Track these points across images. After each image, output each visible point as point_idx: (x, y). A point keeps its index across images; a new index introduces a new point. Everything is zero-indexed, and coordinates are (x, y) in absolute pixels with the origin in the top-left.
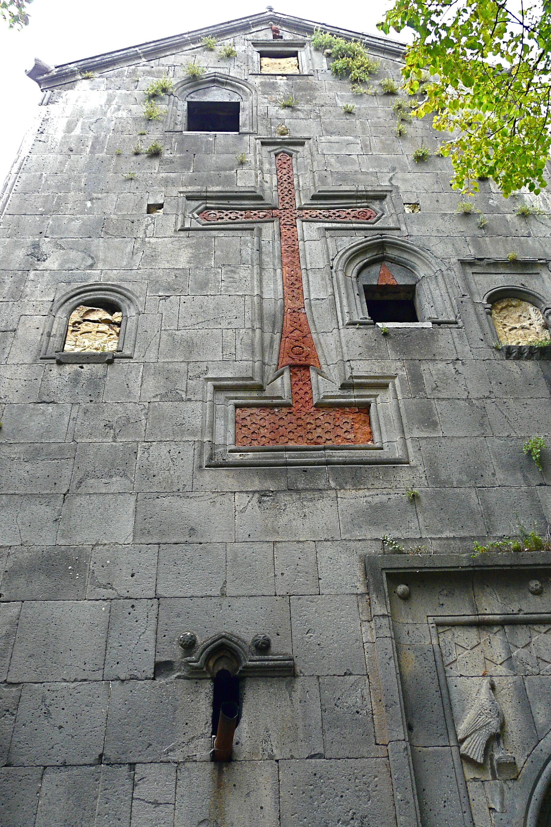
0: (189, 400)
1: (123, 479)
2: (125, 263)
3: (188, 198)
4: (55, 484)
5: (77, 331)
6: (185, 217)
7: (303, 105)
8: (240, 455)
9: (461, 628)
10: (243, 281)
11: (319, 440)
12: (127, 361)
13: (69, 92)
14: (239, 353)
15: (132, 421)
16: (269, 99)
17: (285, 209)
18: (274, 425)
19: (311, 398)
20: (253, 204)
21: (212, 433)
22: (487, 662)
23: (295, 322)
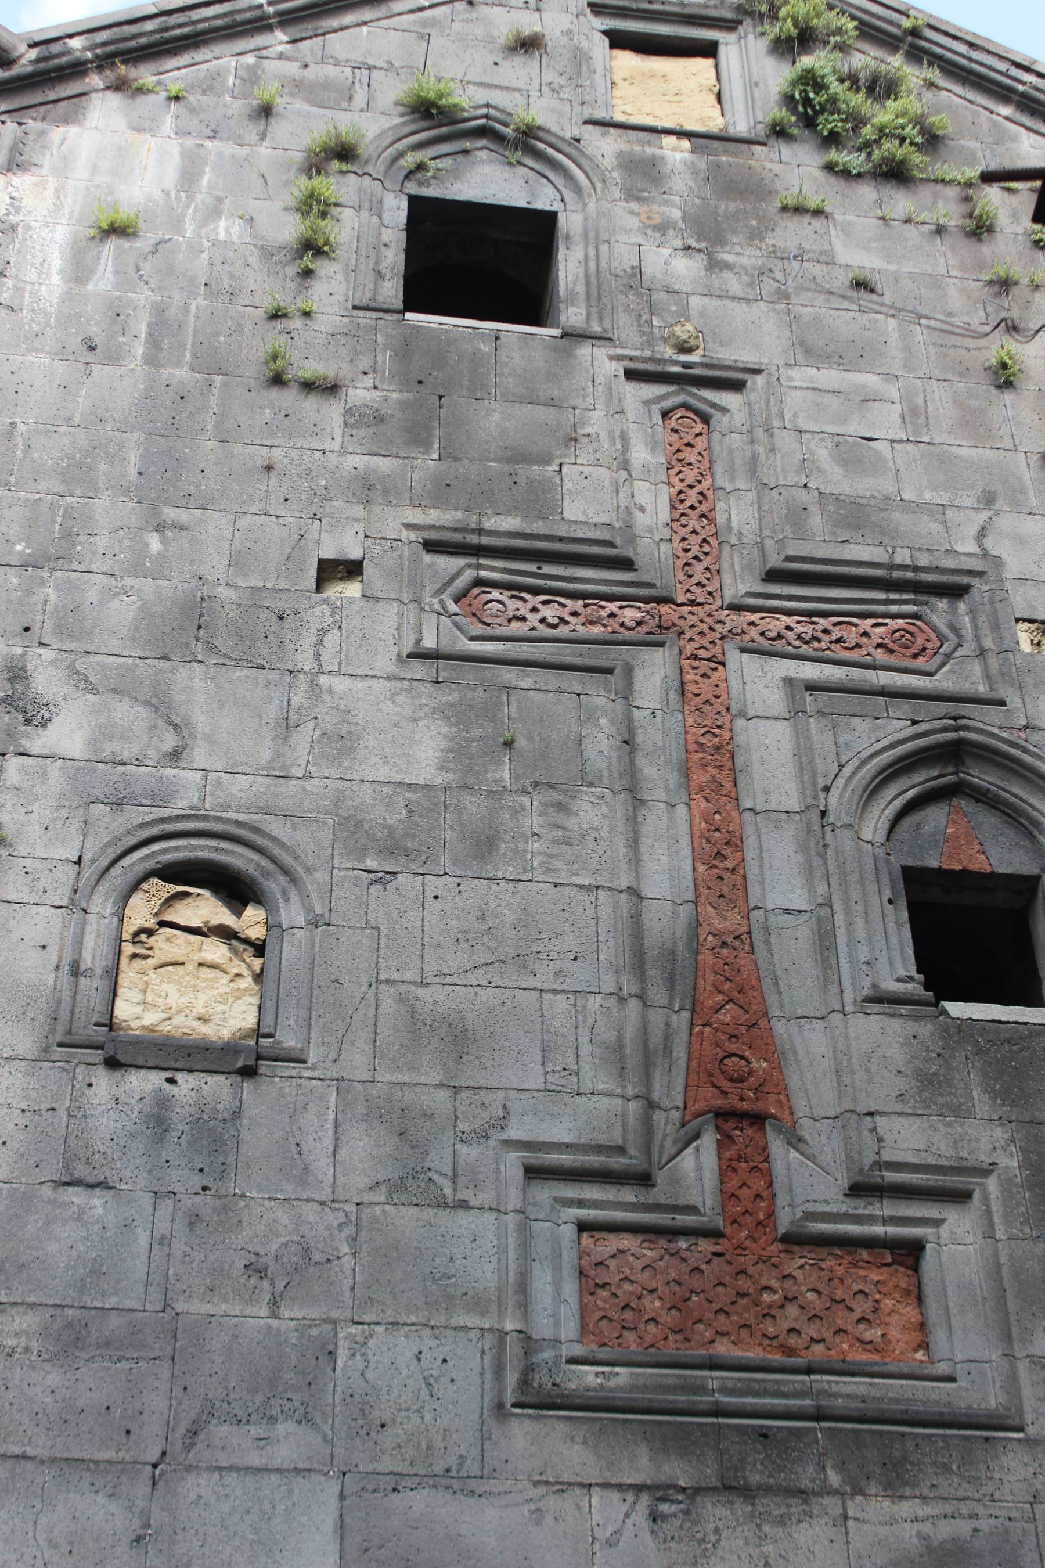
0: (464, 1205)
1: (303, 1429)
2: (266, 755)
3: (431, 546)
4: (128, 1432)
5: (146, 957)
6: (422, 609)
7: (738, 249)
8: (597, 1374)
10: (590, 839)
11: (793, 1341)
12: (294, 1073)
13: (72, 130)
14: (587, 1070)
15: (317, 1257)
16: (644, 216)
17: (693, 603)
18: (677, 1288)
19: (771, 1214)
20: (605, 582)
21: (524, 1306)
23: (728, 979)
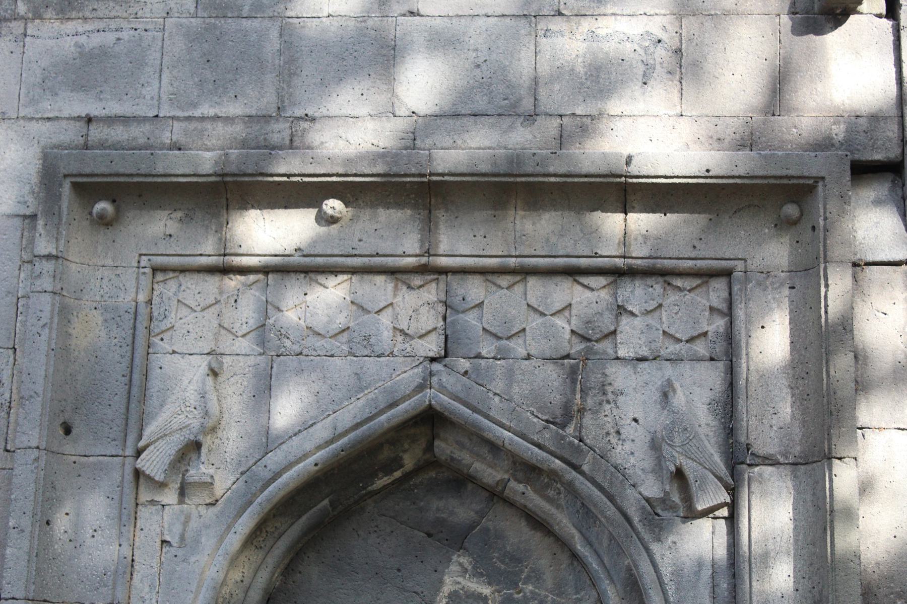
9: (196, 276)
22: (223, 332)
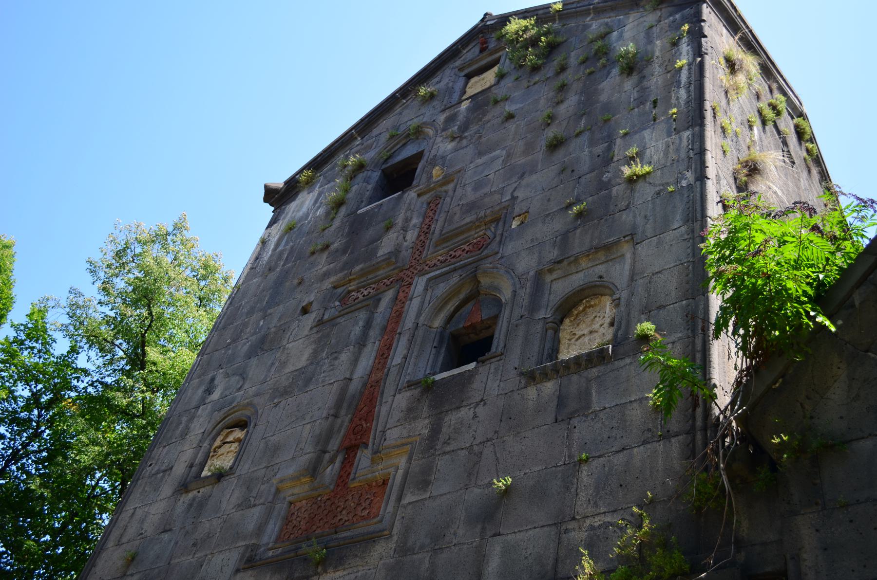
0: (255, 505)
